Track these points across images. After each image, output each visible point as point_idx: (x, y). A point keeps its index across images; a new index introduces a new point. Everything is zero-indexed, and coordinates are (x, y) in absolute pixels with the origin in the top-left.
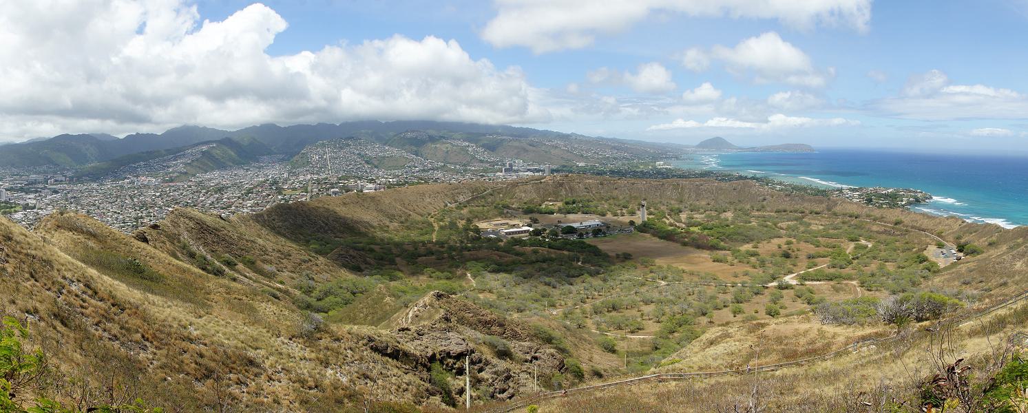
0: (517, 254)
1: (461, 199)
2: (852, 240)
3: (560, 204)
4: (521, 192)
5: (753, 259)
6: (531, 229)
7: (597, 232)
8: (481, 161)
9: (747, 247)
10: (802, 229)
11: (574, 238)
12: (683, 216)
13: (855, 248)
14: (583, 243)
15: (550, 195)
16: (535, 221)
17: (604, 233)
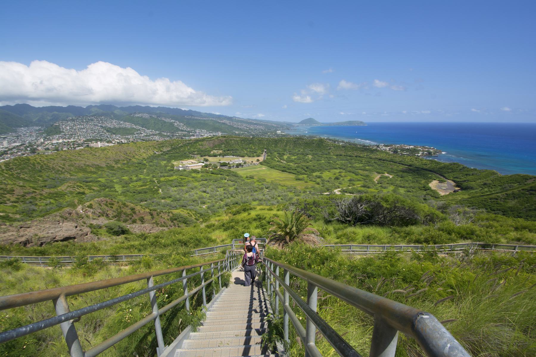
0: (193, 177)
1: (165, 149)
2: (379, 173)
3: (221, 151)
4: (200, 145)
5: (318, 180)
6: (203, 164)
7: (239, 165)
8: (182, 131)
9: (317, 174)
10: (349, 165)
11: (225, 168)
12: (285, 157)
13: (380, 178)
14: (230, 171)
15: (216, 146)
16: (207, 160)
17: (243, 166)
